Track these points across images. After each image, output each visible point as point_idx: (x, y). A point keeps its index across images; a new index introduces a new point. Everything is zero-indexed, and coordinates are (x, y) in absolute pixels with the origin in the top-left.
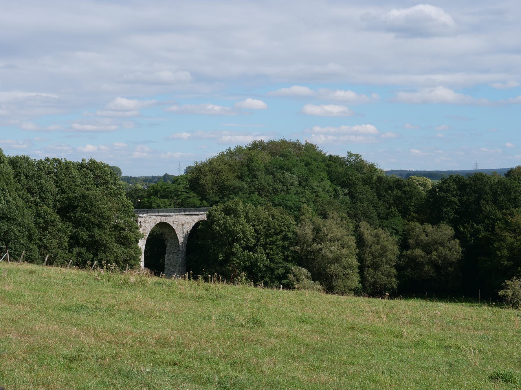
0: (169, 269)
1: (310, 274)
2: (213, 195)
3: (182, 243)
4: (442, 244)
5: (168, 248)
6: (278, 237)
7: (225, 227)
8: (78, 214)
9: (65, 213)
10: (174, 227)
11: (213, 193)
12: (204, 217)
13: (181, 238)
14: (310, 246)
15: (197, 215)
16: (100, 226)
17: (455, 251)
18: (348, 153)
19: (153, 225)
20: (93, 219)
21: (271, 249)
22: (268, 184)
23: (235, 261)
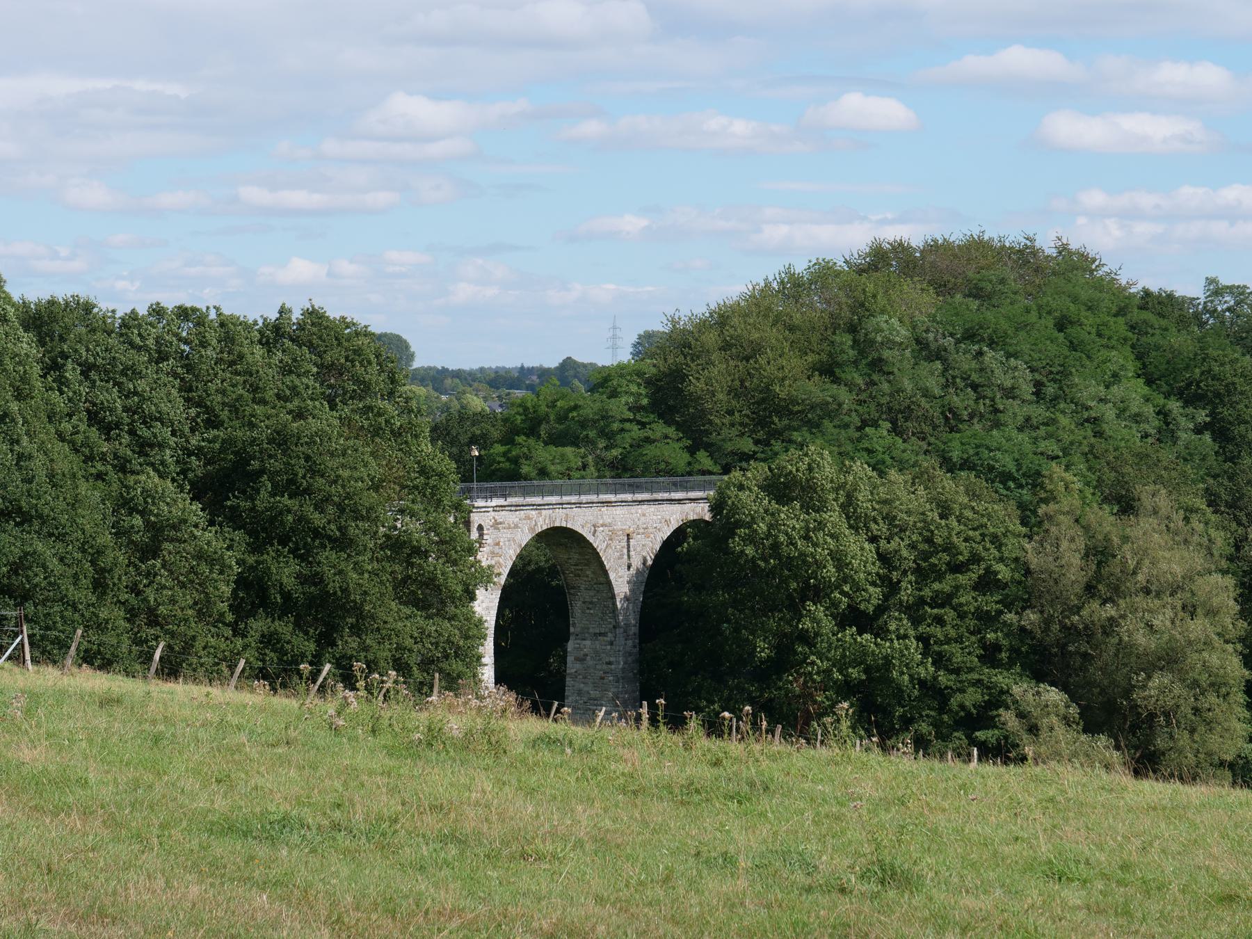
0: (580, 693)
1: (1074, 710)
2: (734, 432)
3: (626, 598)
5: (579, 618)
6: (962, 579)
7: (776, 546)
8: (264, 499)
9: (221, 496)
10: (598, 543)
11: (732, 425)
12: (701, 511)
13: (621, 583)
14: (1077, 610)
15: (679, 501)
16: (343, 543)
18: (1211, 281)
19: (524, 537)
20: (318, 519)
21: (940, 621)
22: (926, 393)
23: (813, 663)
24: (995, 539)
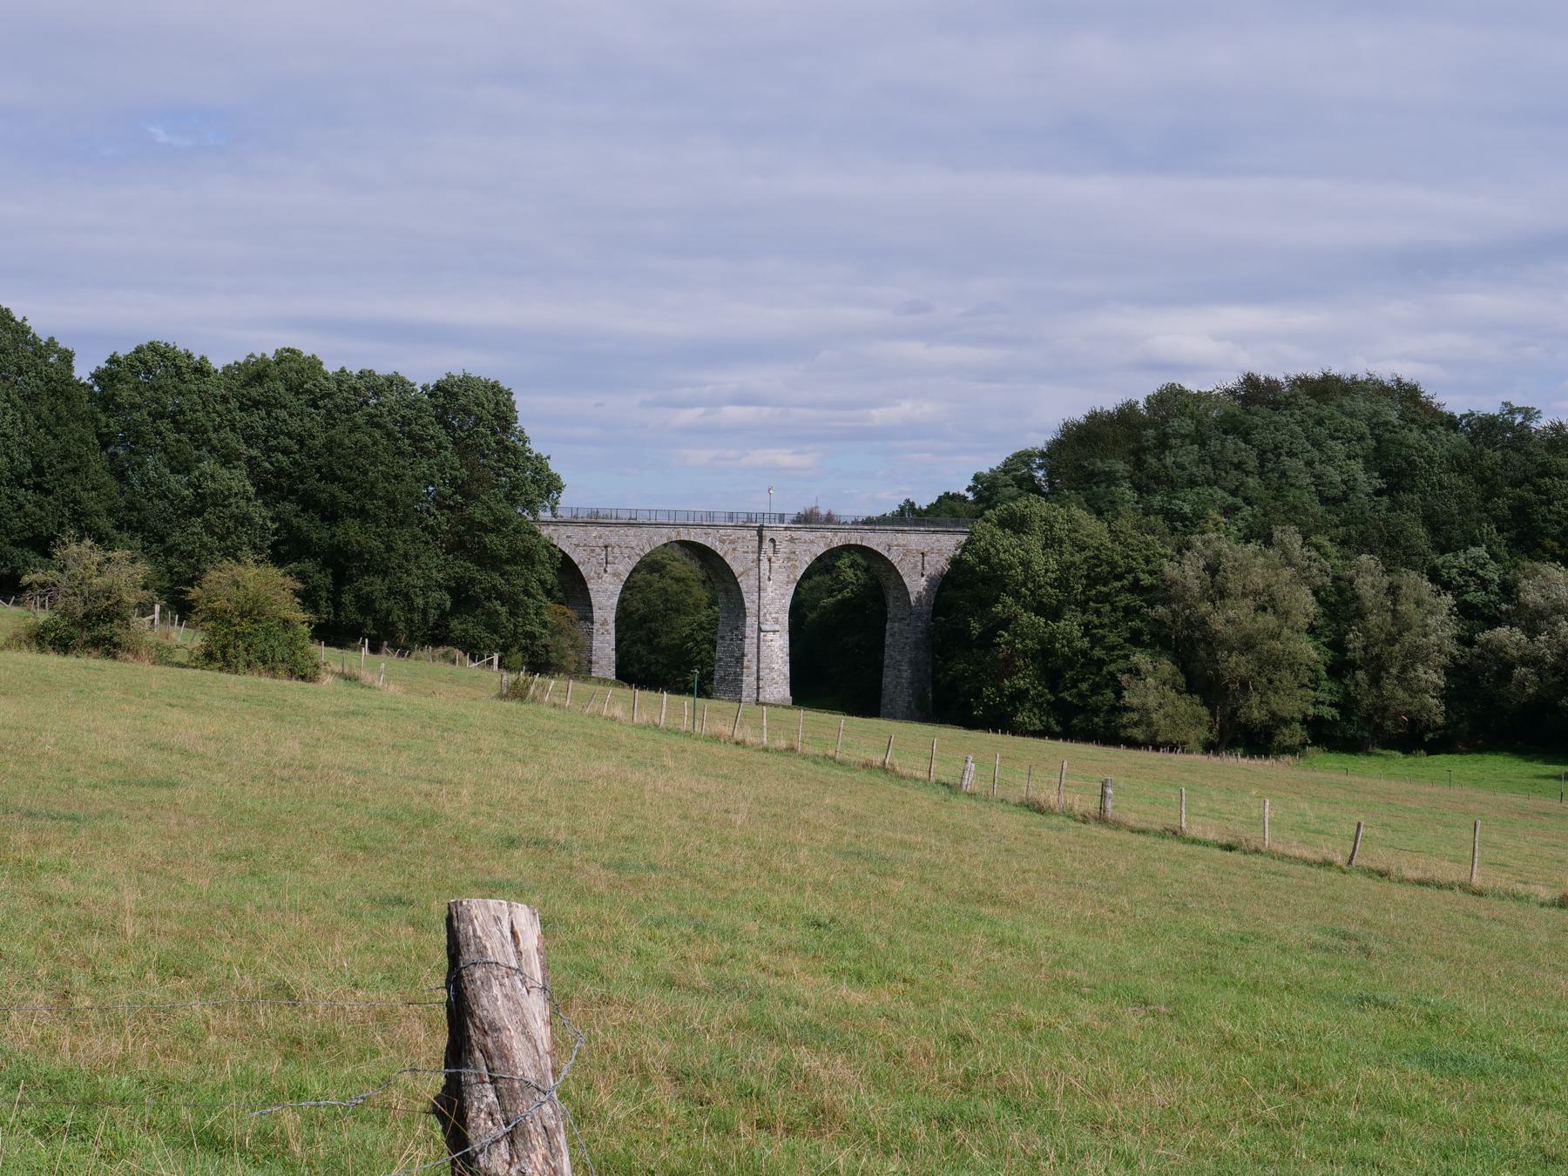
1: (1181, 680)
5: (892, 609)
6: (1118, 584)
10: (894, 557)
12: (963, 538)
13: (916, 585)
19: (820, 549)
21: (1098, 612)
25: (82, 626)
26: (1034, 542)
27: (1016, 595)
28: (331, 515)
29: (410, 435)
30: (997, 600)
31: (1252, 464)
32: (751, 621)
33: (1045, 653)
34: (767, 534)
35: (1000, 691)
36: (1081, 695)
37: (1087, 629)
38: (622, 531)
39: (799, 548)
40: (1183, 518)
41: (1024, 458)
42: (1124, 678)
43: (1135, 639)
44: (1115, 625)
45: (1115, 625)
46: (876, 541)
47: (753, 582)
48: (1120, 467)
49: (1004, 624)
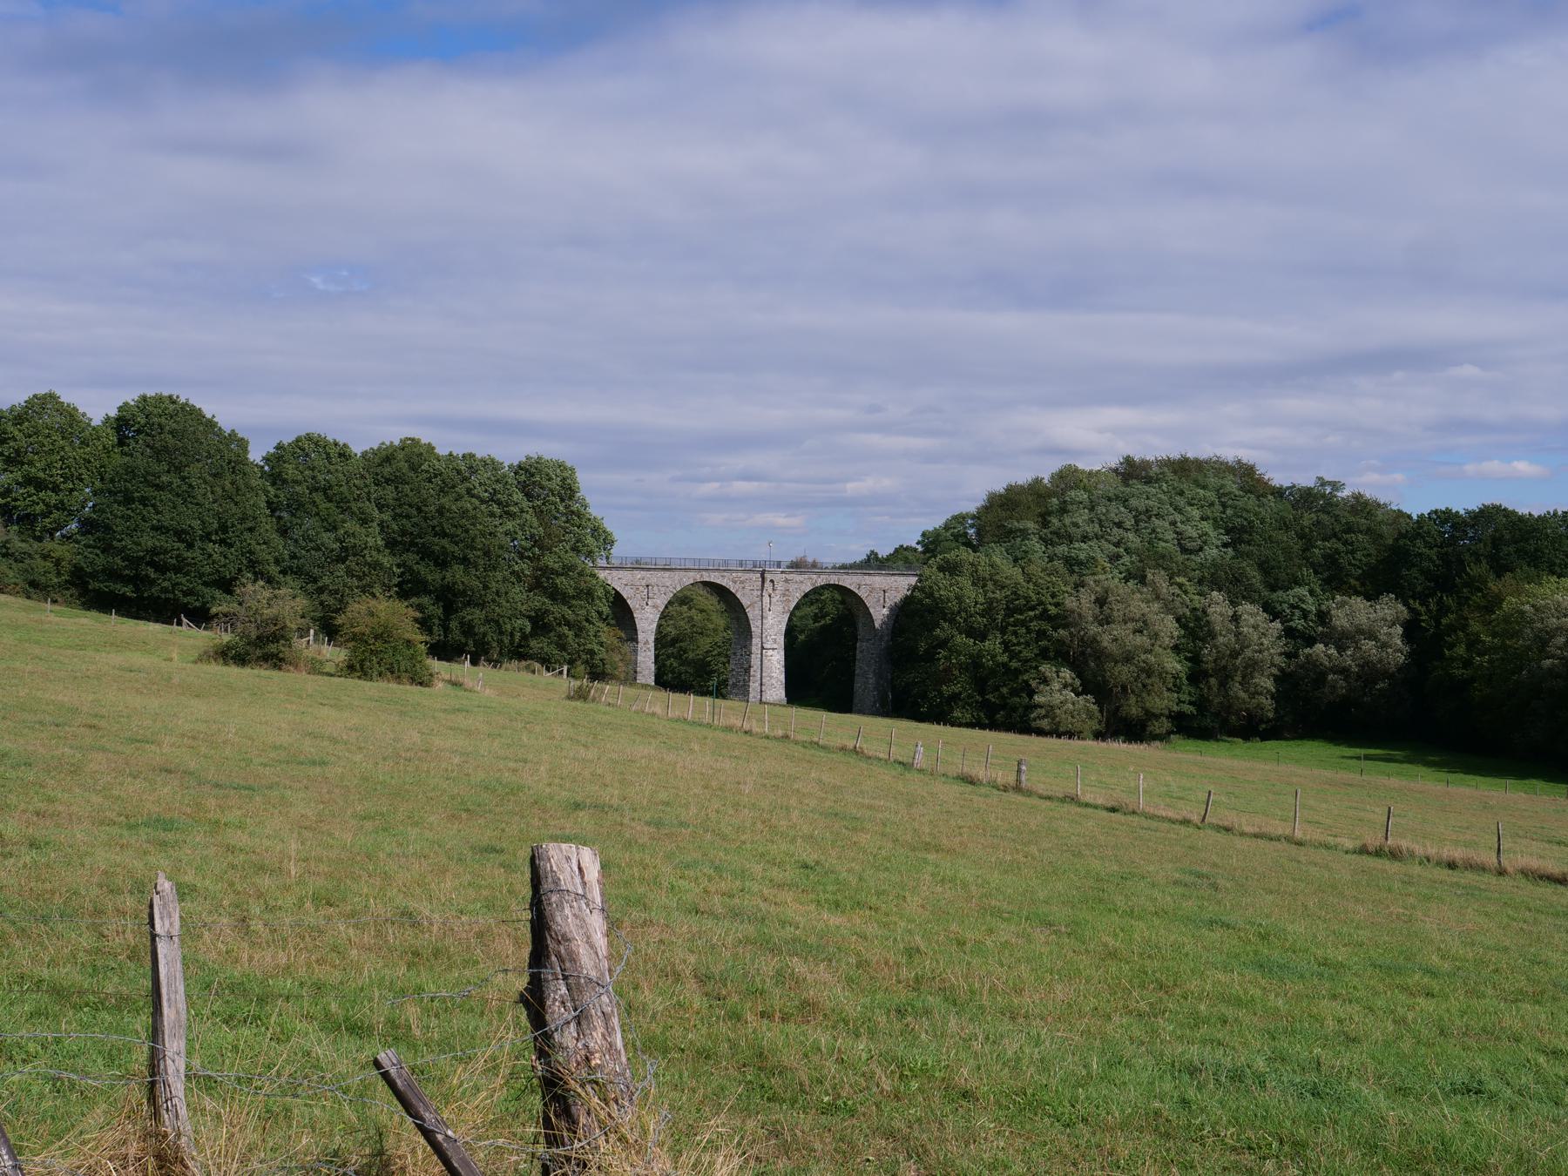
1: (1078, 682)
4: (1372, 636)
5: (861, 632)
6: (1032, 613)
10: (862, 594)
12: (913, 580)
13: (879, 614)
17: (1393, 648)
18: (1319, 478)
21: (1015, 633)
24: (1053, 596)
25: (256, 645)
26: (965, 581)
27: (952, 621)
28: (442, 563)
29: (499, 503)
30: (938, 625)
31: (1129, 523)
32: (756, 641)
33: (975, 663)
34: (768, 576)
35: (940, 693)
36: (1002, 697)
37: (1006, 646)
38: (660, 574)
39: (792, 587)
40: (1080, 563)
41: (960, 519)
42: (1033, 684)
43: (1044, 655)
44: (1027, 644)
45: (1027, 644)
46: (849, 581)
47: (758, 612)
48: (1031, 525)
49: (943, 644)
